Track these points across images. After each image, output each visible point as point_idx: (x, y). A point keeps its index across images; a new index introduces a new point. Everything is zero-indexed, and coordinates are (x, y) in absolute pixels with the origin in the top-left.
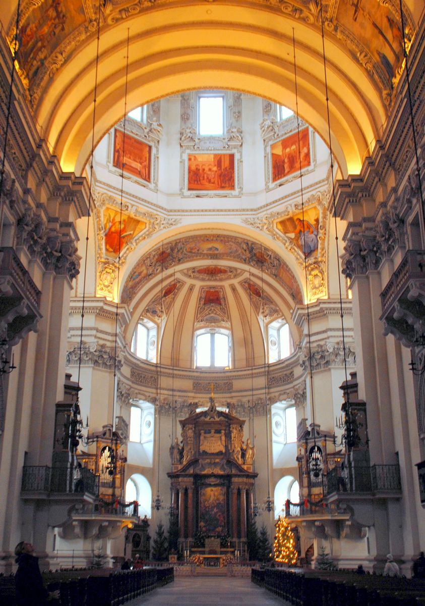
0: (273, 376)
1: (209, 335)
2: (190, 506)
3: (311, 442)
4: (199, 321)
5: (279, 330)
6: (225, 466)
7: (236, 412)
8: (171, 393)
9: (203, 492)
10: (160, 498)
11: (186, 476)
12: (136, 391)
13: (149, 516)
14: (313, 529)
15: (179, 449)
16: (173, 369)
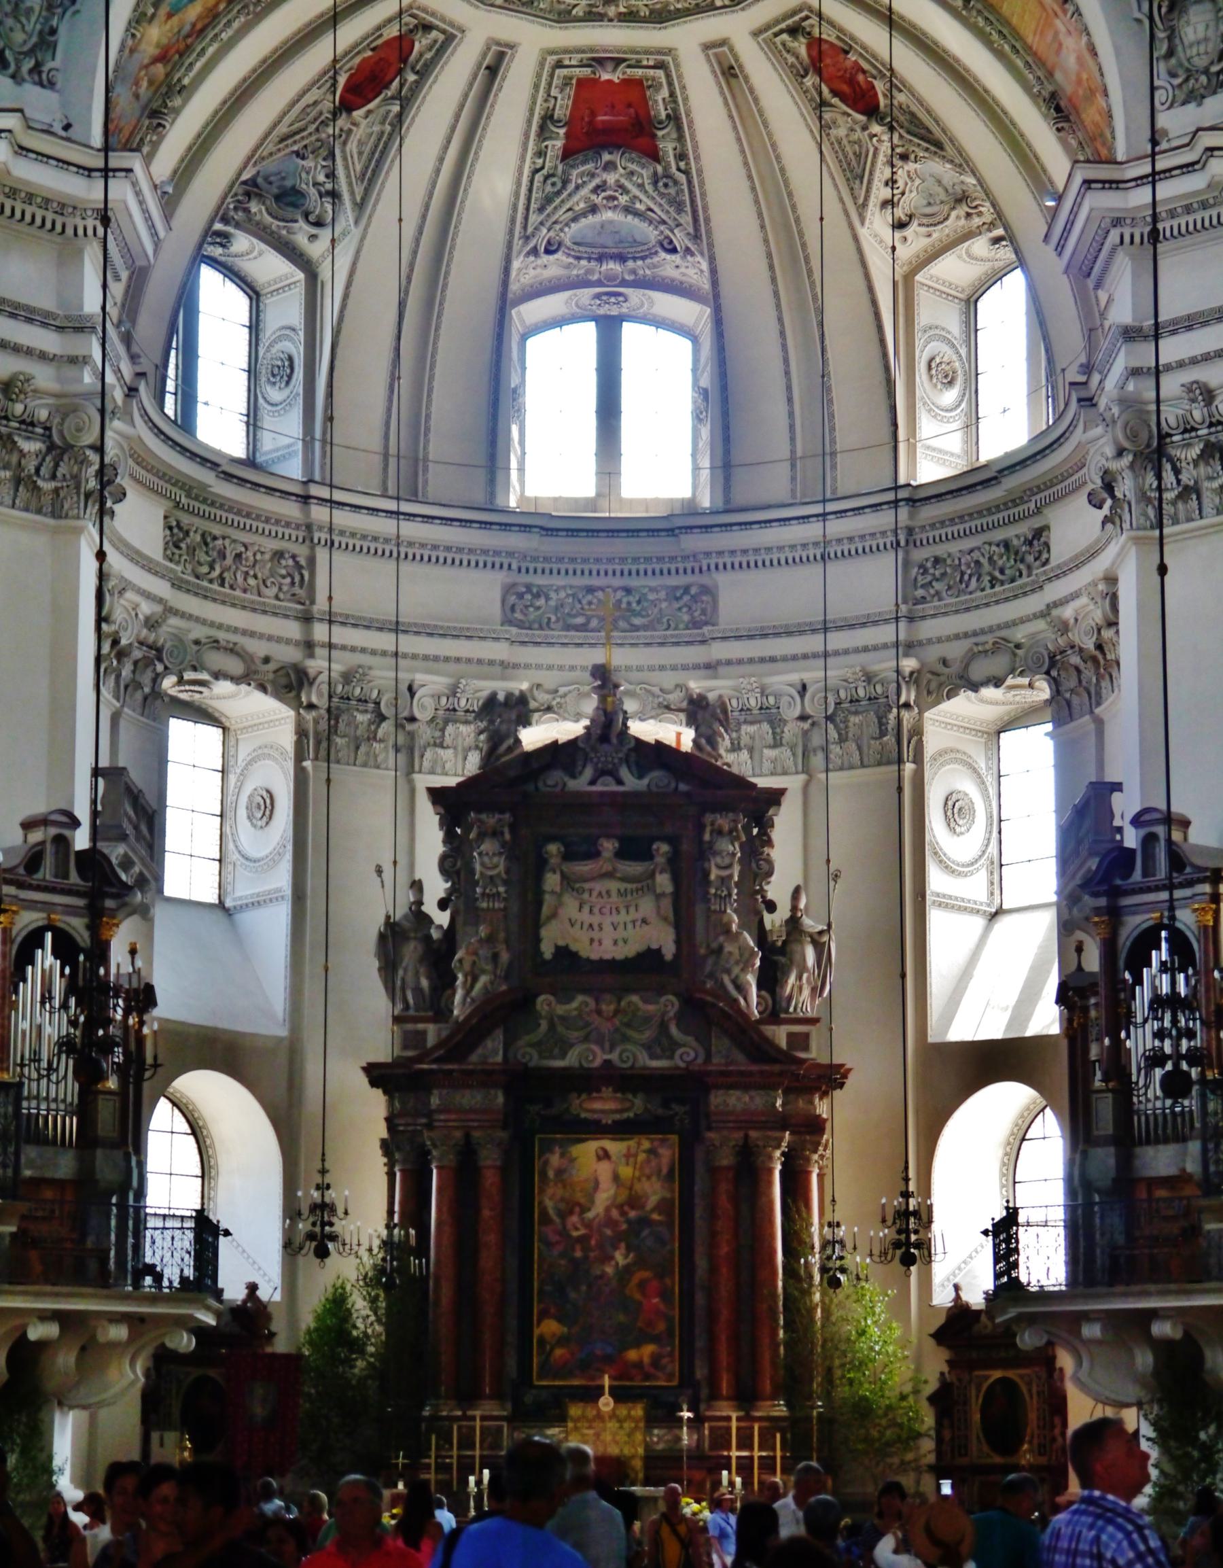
0: (940, 550)
1: (587, 333)
2: (490, 1238)
3: (1136, 909)
4: (534, 252)
5: (970, 303)
6: (674, 1030)
7: (735, 748)
8: (385, 641)
9: (555, 1160)
10: (331, 1195)
11: (469, 1079)
13: (270, 1292)
14: (1144, 1360)
15: (428, 937)
16: (397, 514)
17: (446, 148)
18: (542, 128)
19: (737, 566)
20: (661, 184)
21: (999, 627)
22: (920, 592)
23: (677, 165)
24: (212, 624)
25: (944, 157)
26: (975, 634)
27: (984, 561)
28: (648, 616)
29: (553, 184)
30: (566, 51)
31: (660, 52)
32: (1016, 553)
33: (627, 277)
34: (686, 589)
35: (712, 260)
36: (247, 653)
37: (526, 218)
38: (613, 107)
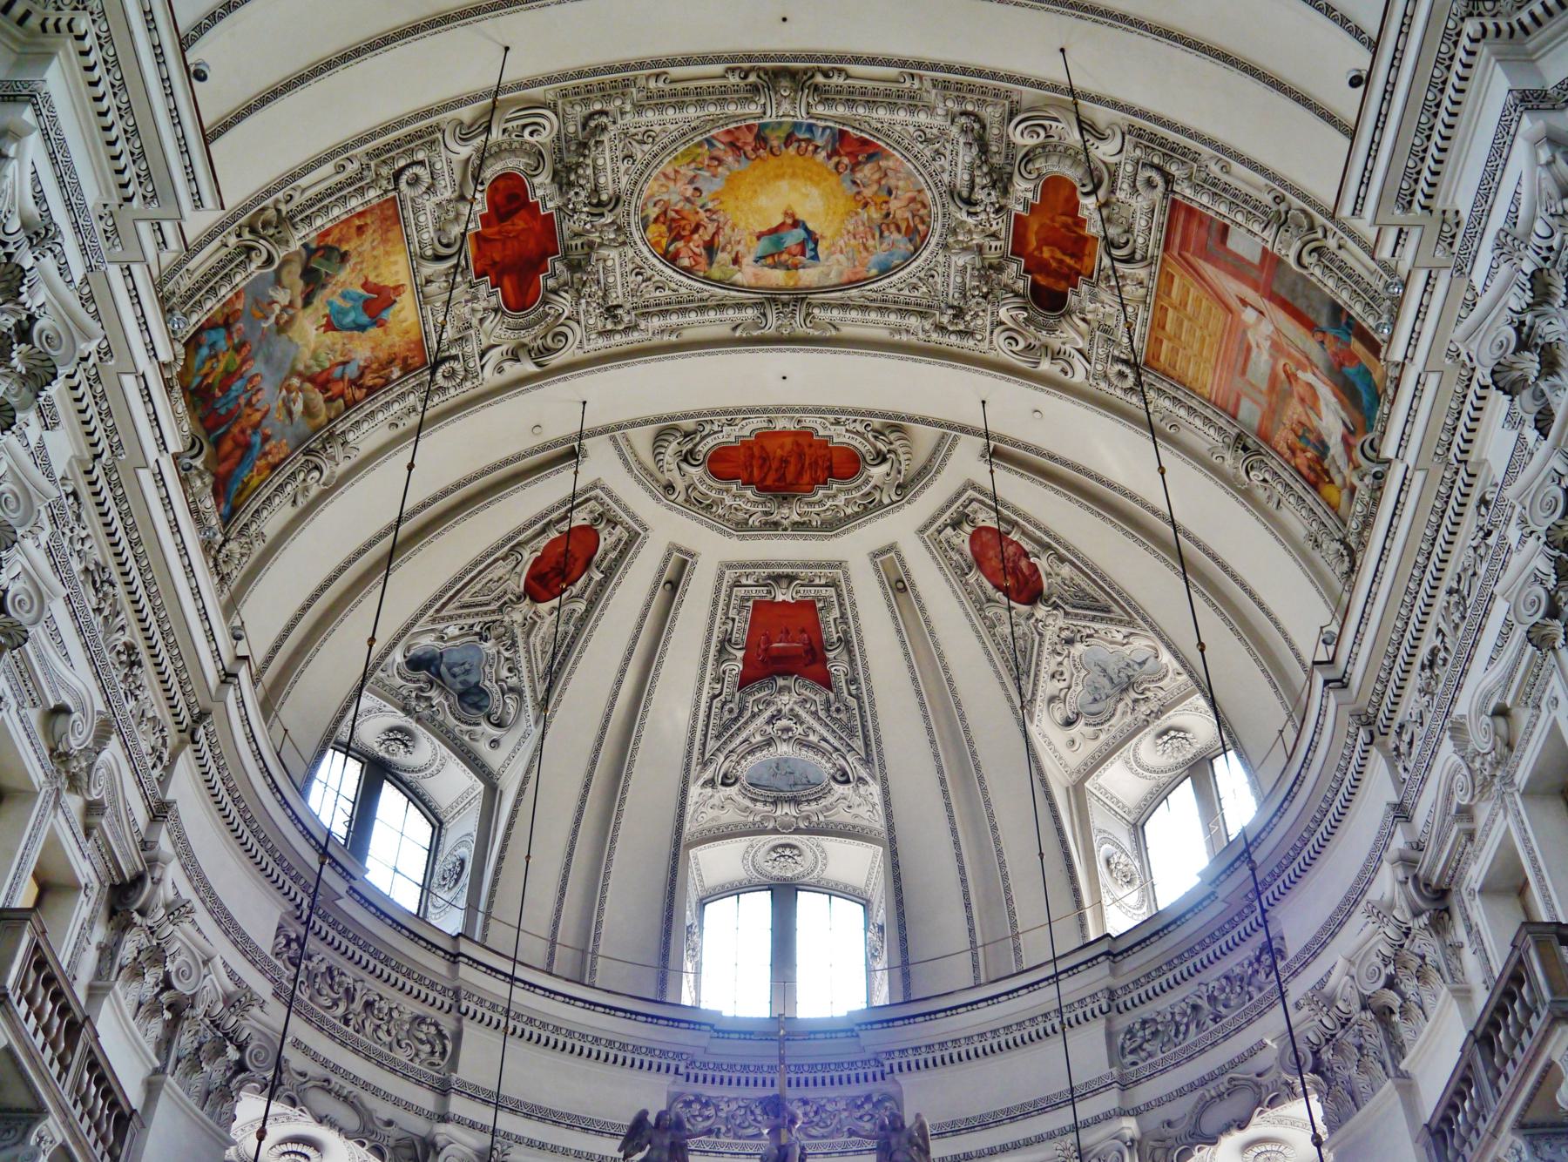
0: (1146, 1011)
4: (711, 782)
5: (1138, 829)
12: (314, 1070)
17: (627, 660)
18: (721, 650)
19: (922, 1064)
20: (833, 709)
21: (1233, 1064)
22: (1130, 1058)
23: (849, 689)
24: (325, 1063)
25: (1112, 620)
26: (1203, 1082)
27: (1204, 1003)
28: (827, 1126)
29: (731, 711)
30: (744, 566)
31: (830, 565)
32: (1242, 980)
33: (802, 826)
34: (868, 1098)
35: (884, 781)
36: (366, 1109)
37: (704, 745)
38: (787, 632)
